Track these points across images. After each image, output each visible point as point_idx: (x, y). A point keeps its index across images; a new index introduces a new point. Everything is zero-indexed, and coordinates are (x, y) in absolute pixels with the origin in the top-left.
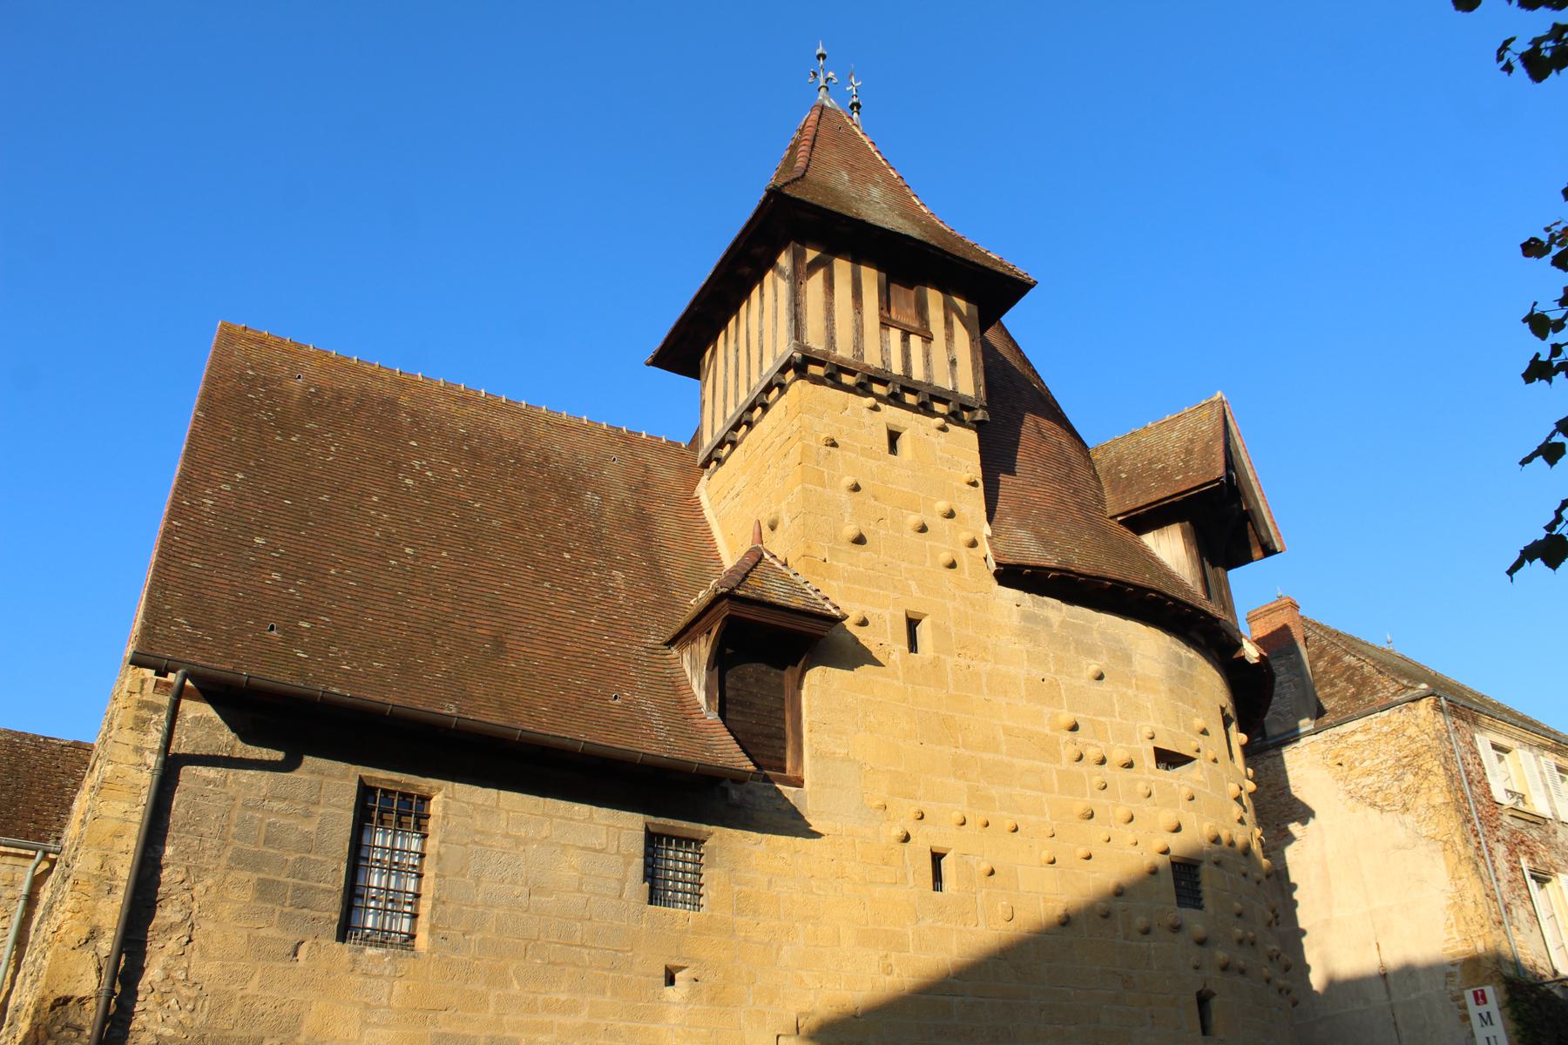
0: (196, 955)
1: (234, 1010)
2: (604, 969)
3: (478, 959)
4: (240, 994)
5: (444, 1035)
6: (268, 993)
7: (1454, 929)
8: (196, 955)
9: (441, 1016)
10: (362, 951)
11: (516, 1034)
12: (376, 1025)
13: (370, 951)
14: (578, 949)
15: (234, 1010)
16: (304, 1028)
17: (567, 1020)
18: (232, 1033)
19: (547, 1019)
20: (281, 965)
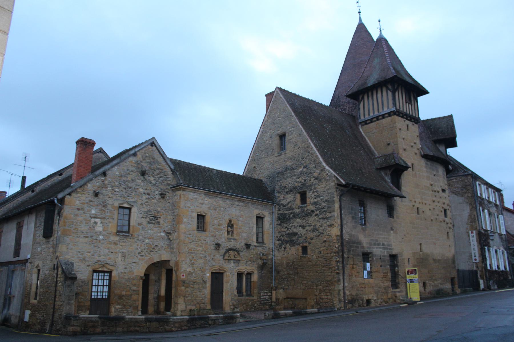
13: (363, 227)
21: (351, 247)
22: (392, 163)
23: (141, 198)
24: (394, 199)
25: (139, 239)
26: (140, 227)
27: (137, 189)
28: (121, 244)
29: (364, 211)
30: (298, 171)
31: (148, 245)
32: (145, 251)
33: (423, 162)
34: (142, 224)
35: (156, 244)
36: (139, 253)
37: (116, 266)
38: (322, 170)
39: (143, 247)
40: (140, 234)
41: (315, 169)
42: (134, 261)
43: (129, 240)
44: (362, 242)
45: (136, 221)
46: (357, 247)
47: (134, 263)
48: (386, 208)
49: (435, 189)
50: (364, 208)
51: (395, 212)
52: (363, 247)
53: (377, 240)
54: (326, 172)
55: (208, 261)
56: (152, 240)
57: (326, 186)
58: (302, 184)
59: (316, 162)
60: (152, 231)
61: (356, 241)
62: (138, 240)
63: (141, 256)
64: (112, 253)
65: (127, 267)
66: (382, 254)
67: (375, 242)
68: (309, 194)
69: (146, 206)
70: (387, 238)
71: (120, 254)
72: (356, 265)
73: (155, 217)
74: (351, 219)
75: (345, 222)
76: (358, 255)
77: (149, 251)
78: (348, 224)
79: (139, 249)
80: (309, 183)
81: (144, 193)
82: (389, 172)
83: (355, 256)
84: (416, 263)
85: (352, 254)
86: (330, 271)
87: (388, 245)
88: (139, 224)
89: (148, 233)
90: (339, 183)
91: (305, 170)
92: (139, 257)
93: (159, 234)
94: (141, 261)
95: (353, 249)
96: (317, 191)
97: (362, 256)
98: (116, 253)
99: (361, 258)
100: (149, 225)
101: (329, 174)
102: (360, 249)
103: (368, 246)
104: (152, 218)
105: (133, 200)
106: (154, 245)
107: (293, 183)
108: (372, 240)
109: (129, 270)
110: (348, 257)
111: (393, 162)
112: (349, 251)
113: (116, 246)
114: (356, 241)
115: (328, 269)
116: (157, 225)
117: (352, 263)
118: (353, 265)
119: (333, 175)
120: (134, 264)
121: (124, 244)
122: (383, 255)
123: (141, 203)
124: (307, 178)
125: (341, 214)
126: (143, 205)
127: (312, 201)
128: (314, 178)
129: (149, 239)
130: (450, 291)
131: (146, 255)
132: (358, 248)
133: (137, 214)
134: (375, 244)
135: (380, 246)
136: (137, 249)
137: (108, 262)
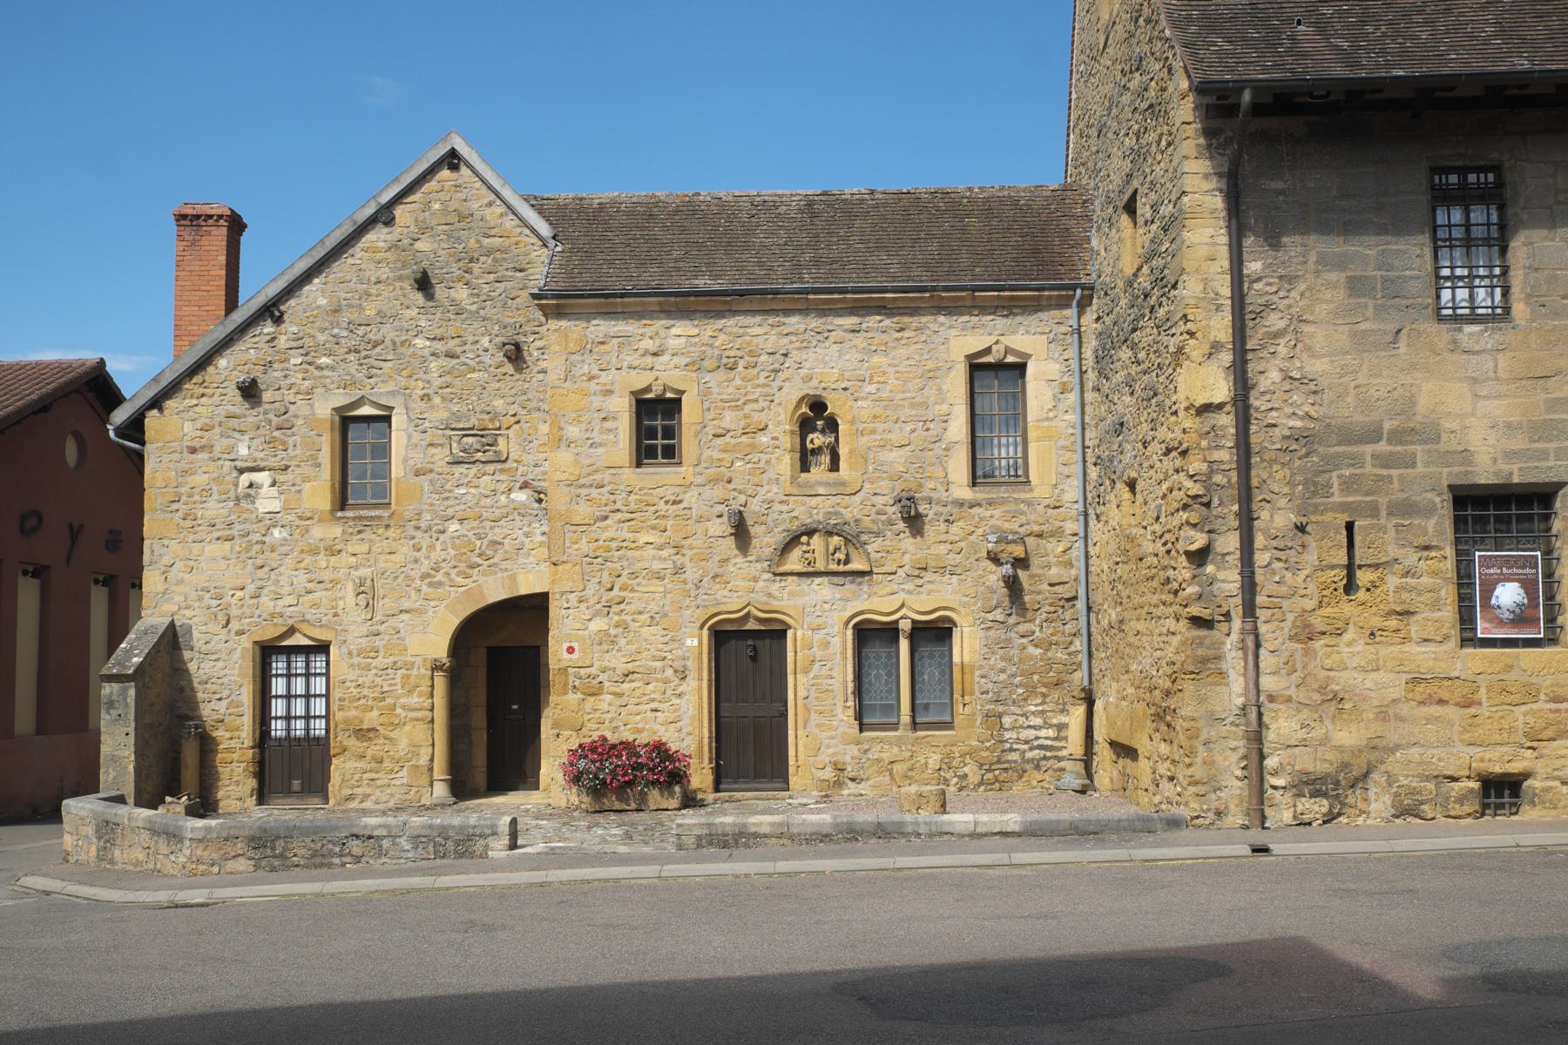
23: (421, 375)
25: (423, 525)
26: (424, 481)
27: (402, 343)
28: (351, 549)
31: (457, 541)
32: (446, 567)
34: (431, 471)
35: (495, 538)
36: (423, 577)
37: (340, 628)
39: (437, 554)
40: (427, 507)
42: (406, 605)
43: (380, 531)
45: (405, 460)
47: (407, 612)
52: (1466, 456)
55: (690, 586)
56: (475, 524)
60: (473, 490)
62: (417, 528)
63: (430, 585)
64: (321, 585)
65: (382, 628)
69: (443, 399)
71: (350, 588)
73: (482, 436)
77: (463, 566)
79: (423, 560)
81: (433, 354)
83: (1375, 513)
85: (1344, 507)
88: (418, 473)
89: (456, 498)
92: (425, 588)
93: (503, 498)
94: (432, 603)
98: (335, 582)
100: (462, 470)
104: (470, 440)
105: (391, 386)
106: (486, 542)
109: (386, 638)
113: (333, 559)
116: (490, 468)
120: (405, 617)
121: (364, 548)
123: (423, 392)
126: (429, 399)
129: (461, 521)
131: (451, 580)
132: (1414, 465)
133: (409, 437)
136: (416, 561)
137: (308, 617)
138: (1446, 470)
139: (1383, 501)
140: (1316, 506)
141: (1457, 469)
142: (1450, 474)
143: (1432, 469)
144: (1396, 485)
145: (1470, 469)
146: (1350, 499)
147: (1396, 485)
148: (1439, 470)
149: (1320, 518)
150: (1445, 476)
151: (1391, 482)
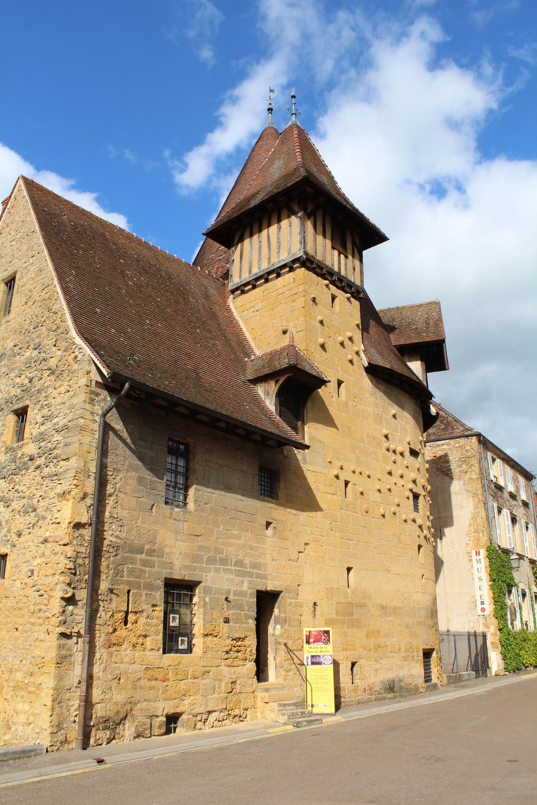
0: (119, 507)
1: (134, 532)
2: (248, 522)
3: (210, 515)
4: (136, 525)
5: (201, 546)
6: (144, 526)
7: (472, 527)
8: (119, 507)
9: (199, 538)
10: (173, 509)
11: (222, 547)
12: (179, 540)
13: (176, 509)
14: (240, 513)
15: (134, 532)
16: (157, 541)
17: (237, 542)
18: (135, 541)
19: (232, 541)
20: (147, 513)
21: (125, 560)
22: (281, 366)
24: (283, 452)
29: (187, 469)
30: (23, 359)
33: (366, 381)
38: (65, 351)
41: (54, 349)
44: (167, 550)
46: (145, 563)
48: (256, 471)
49: (392, 447)
50: (187, 461)
51: (281, 484)
52: (171, 565)
53: (216, 550)
54: (74, 352)
57: (68, 388)
58: (23, 391)
59: (60, 331)
61: (147, 547)
66: (233, 589)
67: (212, 554)
68: (31, 414)
70: (251, 548)
72: (136, 613)
74: (133, 482)
75: (112, 491)
76: (150, 587)
78: (121, 495)
80: (38, 385)
82: (273, 387)
84: (334, 616)
85: (128, 583)
86: (46, 627)
87: (255, 566)
90: (106, 383)
91: (36, 352)
95: (130, 566)
96: (48, 406)
97: (163, 590)
99: (159, 595)
101: (80, 357)
102: (156, 569)
103: (188, 563)
107: (7, 389)
108: (200, 548)
110: (111, 591)
111: (284, 363)
112: (118, 573)
114: (147, 547)
115: (41, 621)
117: (126, 609)
118: (127, 613)
119: (86, 358)
122: (234, 591)
124: (36, 372)
125: (102, 467)
127: (35, 432)
128: (48, 372)
130: (420, 681)
132: (153, 567)
134: (211, 561)
135: (229, 567)
138: (165, 570)
139: (142, 581)
140: (117, 580)
141: (169, 571)
142: (165, 573)
143: (160, 569)
144: (147, 575)
145: (173, 571)
146: (130, 579)
147: (147, 575)
148: (162, 570)
149: (118, 587)
150: (164, 573)
151: (145, 573)
